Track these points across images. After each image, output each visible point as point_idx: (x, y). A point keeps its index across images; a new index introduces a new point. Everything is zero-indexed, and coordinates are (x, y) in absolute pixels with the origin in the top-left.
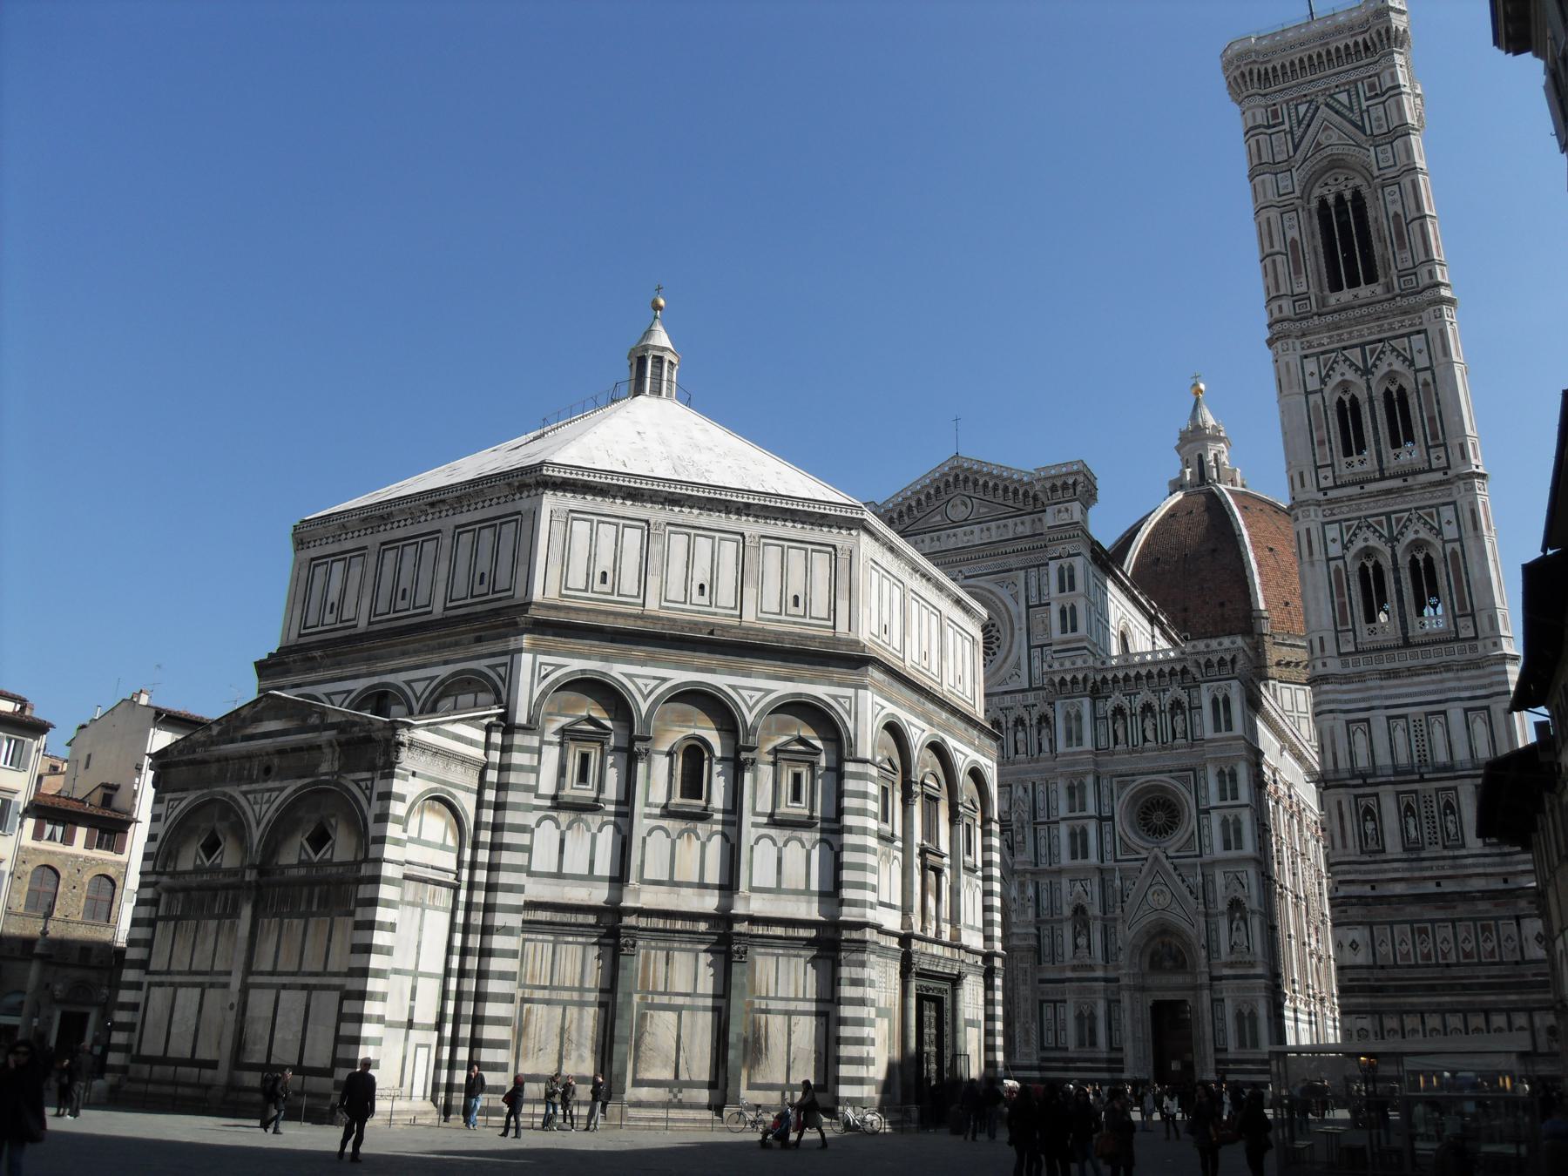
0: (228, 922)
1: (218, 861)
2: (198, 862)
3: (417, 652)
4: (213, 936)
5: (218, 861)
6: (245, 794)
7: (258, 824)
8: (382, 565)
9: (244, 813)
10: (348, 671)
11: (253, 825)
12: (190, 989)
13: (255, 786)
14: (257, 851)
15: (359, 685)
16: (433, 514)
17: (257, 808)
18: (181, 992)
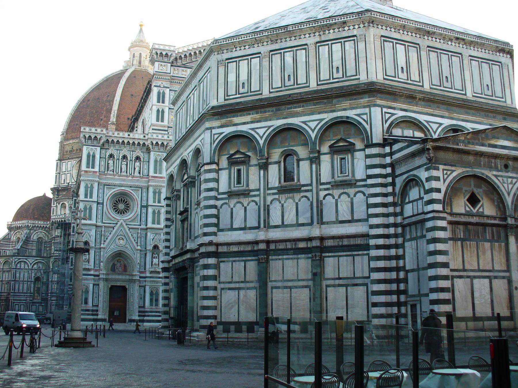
0: (496, 244)
1: (481, 210)
2: (468, 209)
3: (473, 115)
4: (489, 252)
5: (481, 210)
6: (496, 176)
7: (509, 194)
8: (429, 58)
9: (498, 187)
10: (437, 112)
11: (506, 195)
12: (482, 279)
13: (500, 173)
14: (512, 209)
15: (447, 122)
16: (455, 43)
17: (506, 185)
18: (476, 281)
